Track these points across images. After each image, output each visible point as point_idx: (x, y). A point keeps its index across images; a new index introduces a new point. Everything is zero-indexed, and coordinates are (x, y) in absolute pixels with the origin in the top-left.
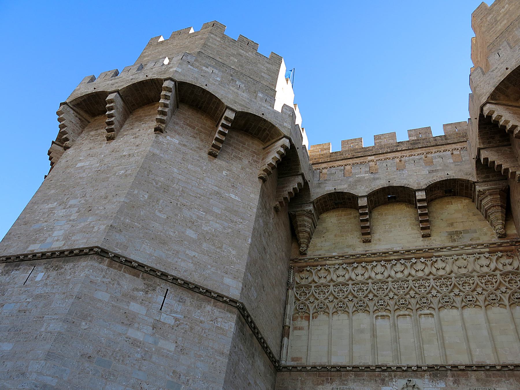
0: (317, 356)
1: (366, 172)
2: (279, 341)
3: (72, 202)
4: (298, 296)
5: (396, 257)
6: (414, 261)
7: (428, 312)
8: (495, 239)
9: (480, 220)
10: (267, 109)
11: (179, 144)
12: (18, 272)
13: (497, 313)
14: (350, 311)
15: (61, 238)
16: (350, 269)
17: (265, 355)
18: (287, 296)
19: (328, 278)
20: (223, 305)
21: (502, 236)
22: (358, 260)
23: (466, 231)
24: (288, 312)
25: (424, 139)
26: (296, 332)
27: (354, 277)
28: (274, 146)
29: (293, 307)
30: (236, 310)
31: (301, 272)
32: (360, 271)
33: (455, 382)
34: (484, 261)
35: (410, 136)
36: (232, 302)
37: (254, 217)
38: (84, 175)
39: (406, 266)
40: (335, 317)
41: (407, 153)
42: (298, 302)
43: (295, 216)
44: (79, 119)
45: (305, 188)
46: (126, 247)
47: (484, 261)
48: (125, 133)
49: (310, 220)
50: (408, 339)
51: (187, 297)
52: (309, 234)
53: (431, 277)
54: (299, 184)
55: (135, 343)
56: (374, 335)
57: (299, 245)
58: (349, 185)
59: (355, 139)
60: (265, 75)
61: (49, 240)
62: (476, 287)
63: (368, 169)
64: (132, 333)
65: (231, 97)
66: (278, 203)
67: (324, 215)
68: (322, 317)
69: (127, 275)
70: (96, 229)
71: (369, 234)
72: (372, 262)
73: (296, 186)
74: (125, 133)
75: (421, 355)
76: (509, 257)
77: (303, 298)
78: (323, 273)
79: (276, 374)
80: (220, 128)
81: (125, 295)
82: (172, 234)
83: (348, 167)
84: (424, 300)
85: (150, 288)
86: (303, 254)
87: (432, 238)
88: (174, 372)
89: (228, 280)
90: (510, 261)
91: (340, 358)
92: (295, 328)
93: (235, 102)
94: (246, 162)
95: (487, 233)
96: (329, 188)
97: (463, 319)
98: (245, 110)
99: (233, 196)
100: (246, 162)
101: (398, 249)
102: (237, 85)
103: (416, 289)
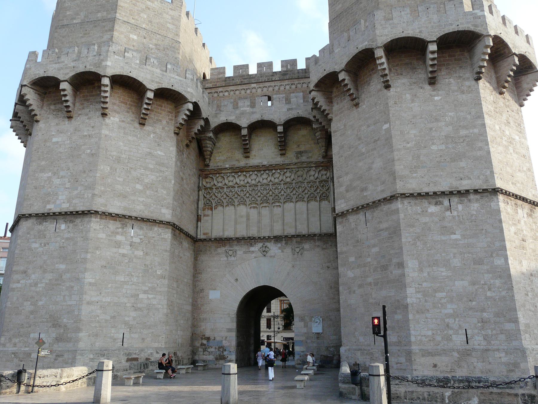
1: (248, 106)
2: (195, 226)
3: (62, 173)
4: (205, 195)
5: (264, 169)
6: (274, 171)
7: (278, 204)
8: (320, 159)
9: (315, 143)
10: (176, 79)
11: (120, 121)
12: (47, 223)
13: (314, 205)
14: (236, 205)
15: (66, 201)
16: (236, 176)
17: (188, 238)
18: (199, 195)
19: (223, 183)
20: (163, 225)
21: (324, 157)
23: (306, 152)
24: (200, 206)
25: (291, 71)
26: (205, 218)
28: (182, 107)
29: (203, 203)
30: (171, 227)
31: (206, 178)
32: (242, 178)
33: (286, 244)
35: (282, 66)
36: (168, 223)
37: (174, 164)
38: (61, 150)
39: (269, 175)
40: (227, 208)
41: (278, 83)
42: (205, 199)
43: (201, 140)
44: (38, 94)
45: (207, 121)
46: (106, 206)
47: (312, 173)
48: (80, 112)
49: (211, 143)
50: (266, 220)
51: (143, 225)
52: (210, 152)
53: (282, 182)
54: (201, 126)
55: (124, 255)
56: (248, 219)
57: (204, 160)
58: (236, 117)
59: (243, 65)
60: (169, 25)
61: (58, 202)
62: (305, 189)
63: (249, 103)
64: (122, 251)
65: (149, 77)
66: (188, 141)
68: (220, 208)
69: (111, 221)
70: (86, 196)
71: (249, 152)
72: (250, 171)
73: (200, 128)
74: (80, 112)
75: (272, 230)
76: (326, 170)
77: (208, 196)
78: (220, 179)
79: (195, 243)
80: (145, 106)
81: (113, 233)
82: (128, 190)
83: (237, 92)
84: (277, 197)
85: (124, 226)
86: (208, 166)
87: (287, 155)
88: (145, 265)
89: (164, 211)
90: (326, 172)
91: (229, 233)
92: (204, 215)
93: (153, 81)
94: (164, 122)
95: (317, 155)
96: (223, 118)
97: (295, 208)
98: (161, 86)
99: (159, 153)
101: (265, 163)
102: (151, 63)
103: (273, 191)
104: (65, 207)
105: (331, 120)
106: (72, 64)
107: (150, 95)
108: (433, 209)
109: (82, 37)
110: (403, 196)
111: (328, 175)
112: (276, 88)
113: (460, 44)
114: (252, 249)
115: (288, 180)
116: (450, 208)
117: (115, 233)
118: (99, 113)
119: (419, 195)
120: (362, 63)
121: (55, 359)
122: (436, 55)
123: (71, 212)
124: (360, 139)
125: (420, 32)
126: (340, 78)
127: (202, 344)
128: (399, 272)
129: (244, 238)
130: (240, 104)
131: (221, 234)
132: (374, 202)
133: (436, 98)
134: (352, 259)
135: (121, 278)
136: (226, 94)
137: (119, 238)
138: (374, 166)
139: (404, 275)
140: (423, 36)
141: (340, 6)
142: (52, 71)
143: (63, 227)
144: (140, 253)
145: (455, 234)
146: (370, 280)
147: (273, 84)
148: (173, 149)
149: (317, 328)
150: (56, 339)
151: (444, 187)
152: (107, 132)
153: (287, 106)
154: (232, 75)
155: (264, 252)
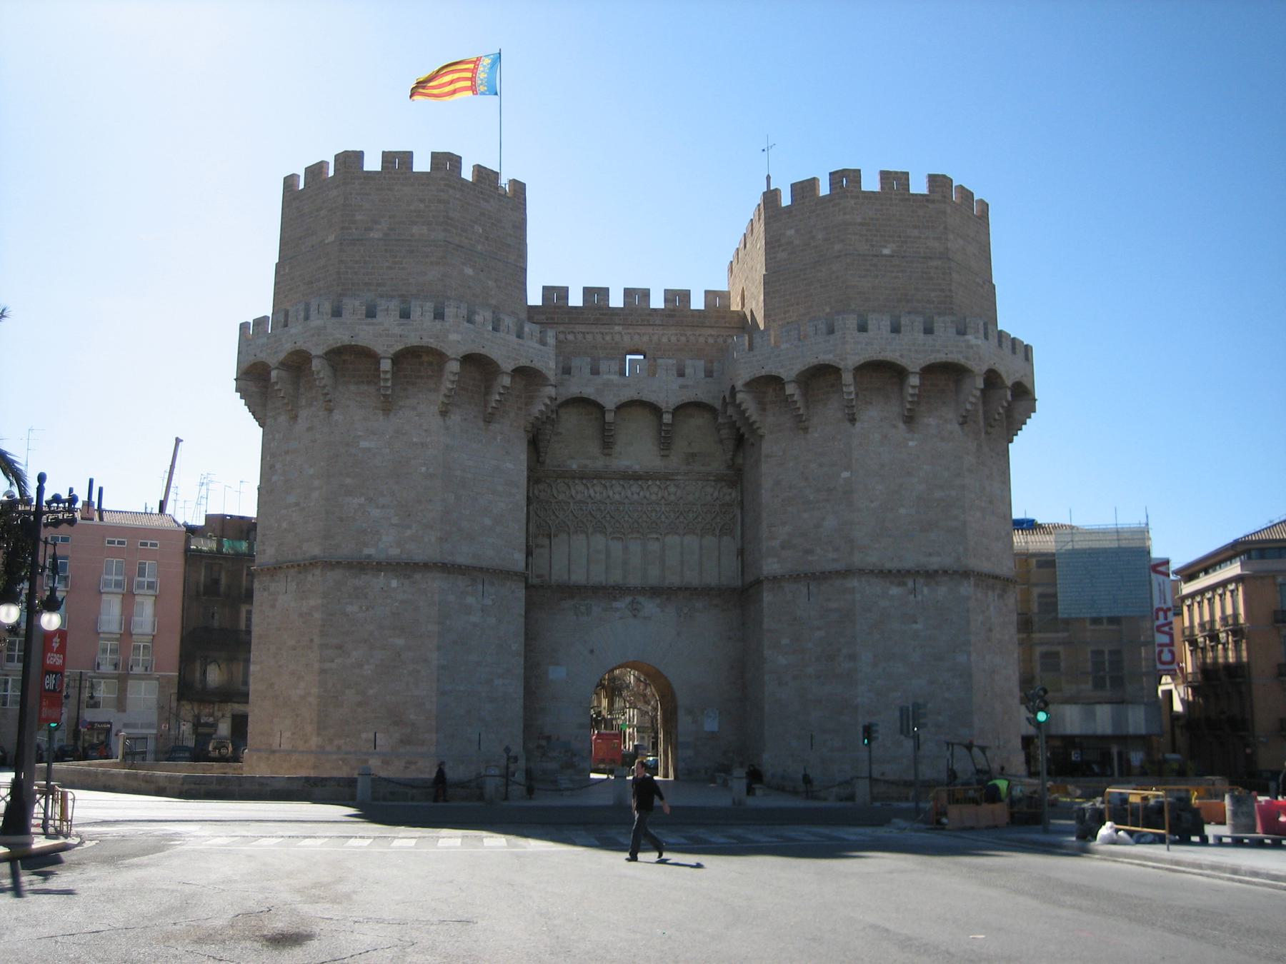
0: (559, 573)
1: (615, 373)
14: (590, 530)
21: (729, 467)
22: (597, 476)
34: (710, 490)
35: (666, 301)
63: (617, 368)
80: (497, 397)
83: (589, 337)
86: (544, 463)
91: (578, 577)
92: (537, 546)
96: (575, 388)
99: (510, 466)
101: (637, 467)
104: (394, 552)
105: (762, 437)
106: (397, 330)
107: (507, 381)
108: (895, 591)
109: (390, 268)
110: (862, 572)
111: (734, 495)
112: (655, 338)
113: (947, 374)
114: (616, 604)
115: (672, 498)
116: (914, 591)
118: (435, 409)
119: (881, 571)
120: (820, 377)
121: (406, 768)
122: (917, 391)
123: (407, 564)
125: (901, 356)
126: (788, 392)
127: (539, 747)
129: (604, 588)
130: (603, 366)
131: (566, 577)
132: (823, 573)
133: (911, 443)
134: (785, 641)
136: (570, 337)
137: (470, 600)
140: (904, 362)
142: (366, 335)
143: (394, 583)
145: (916, 622)
147: (650, 330)
148: (524, 457)
149: (711, 724)
150: (402, 741)
151: (909, 563)
153: (681, 381)
154: (580, 304)
155: (635, 610)
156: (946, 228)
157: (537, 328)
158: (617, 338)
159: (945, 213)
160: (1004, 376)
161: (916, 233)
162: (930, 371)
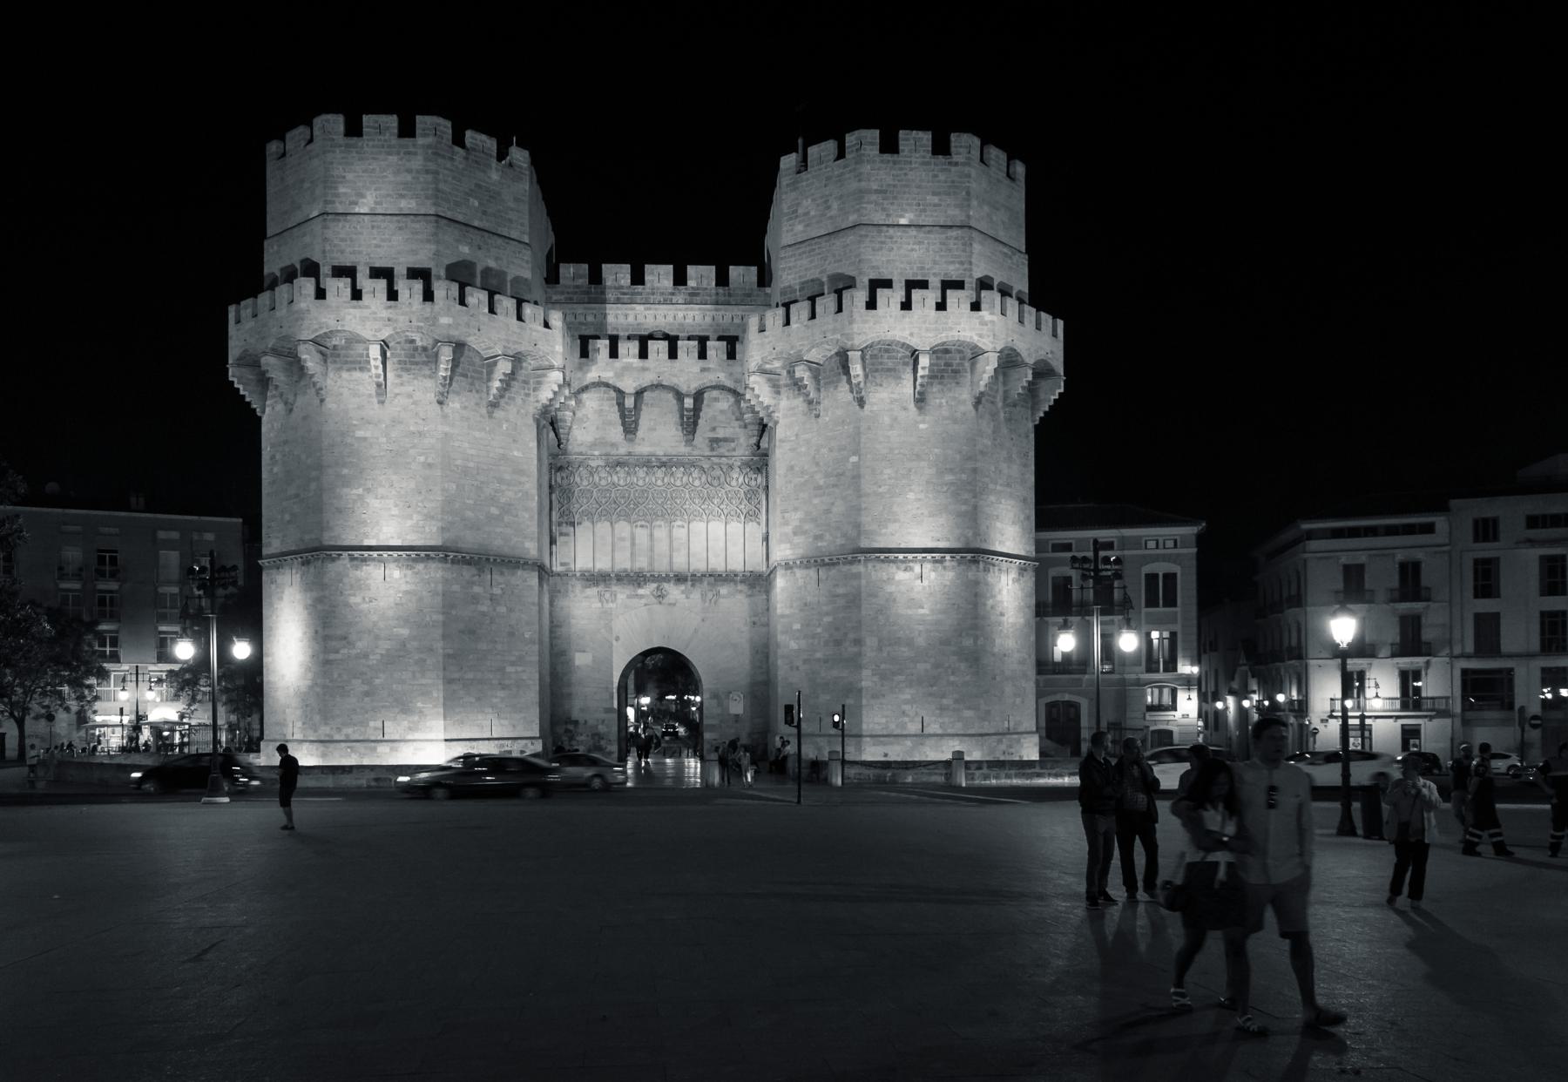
3: (381, 491)
27: (615, 478)
36: (534, 564)
40: (599, 525)
55: (484, 614)
56: (633, 544)
67: (585, 396)
68: (587, 524)
75: (671, 562)
85: (481, 571)
100: (519, 401)
114: (641, 591)
117: (471, 583)
118: (431, 397)
124: (817, 464)
126: (798, 375)
128: (856, 649)
131: (590, 566)
133: (922, 426)
135: (483, 646)
137: (477, 589)
138: (835, 509)
139: (859, 654)
141: (800, 228)
143: (397, 574)
144: (502, 609)
146: (818, 655)
152: (447, 429)
153: (702, 363)
155: (660, 596)
156: (968, 193)
157: (540, 311)
158: (641, 319)
159: (969, 176)
160: (1024, 354)
161: (936, 200)
162: (941, 352)
